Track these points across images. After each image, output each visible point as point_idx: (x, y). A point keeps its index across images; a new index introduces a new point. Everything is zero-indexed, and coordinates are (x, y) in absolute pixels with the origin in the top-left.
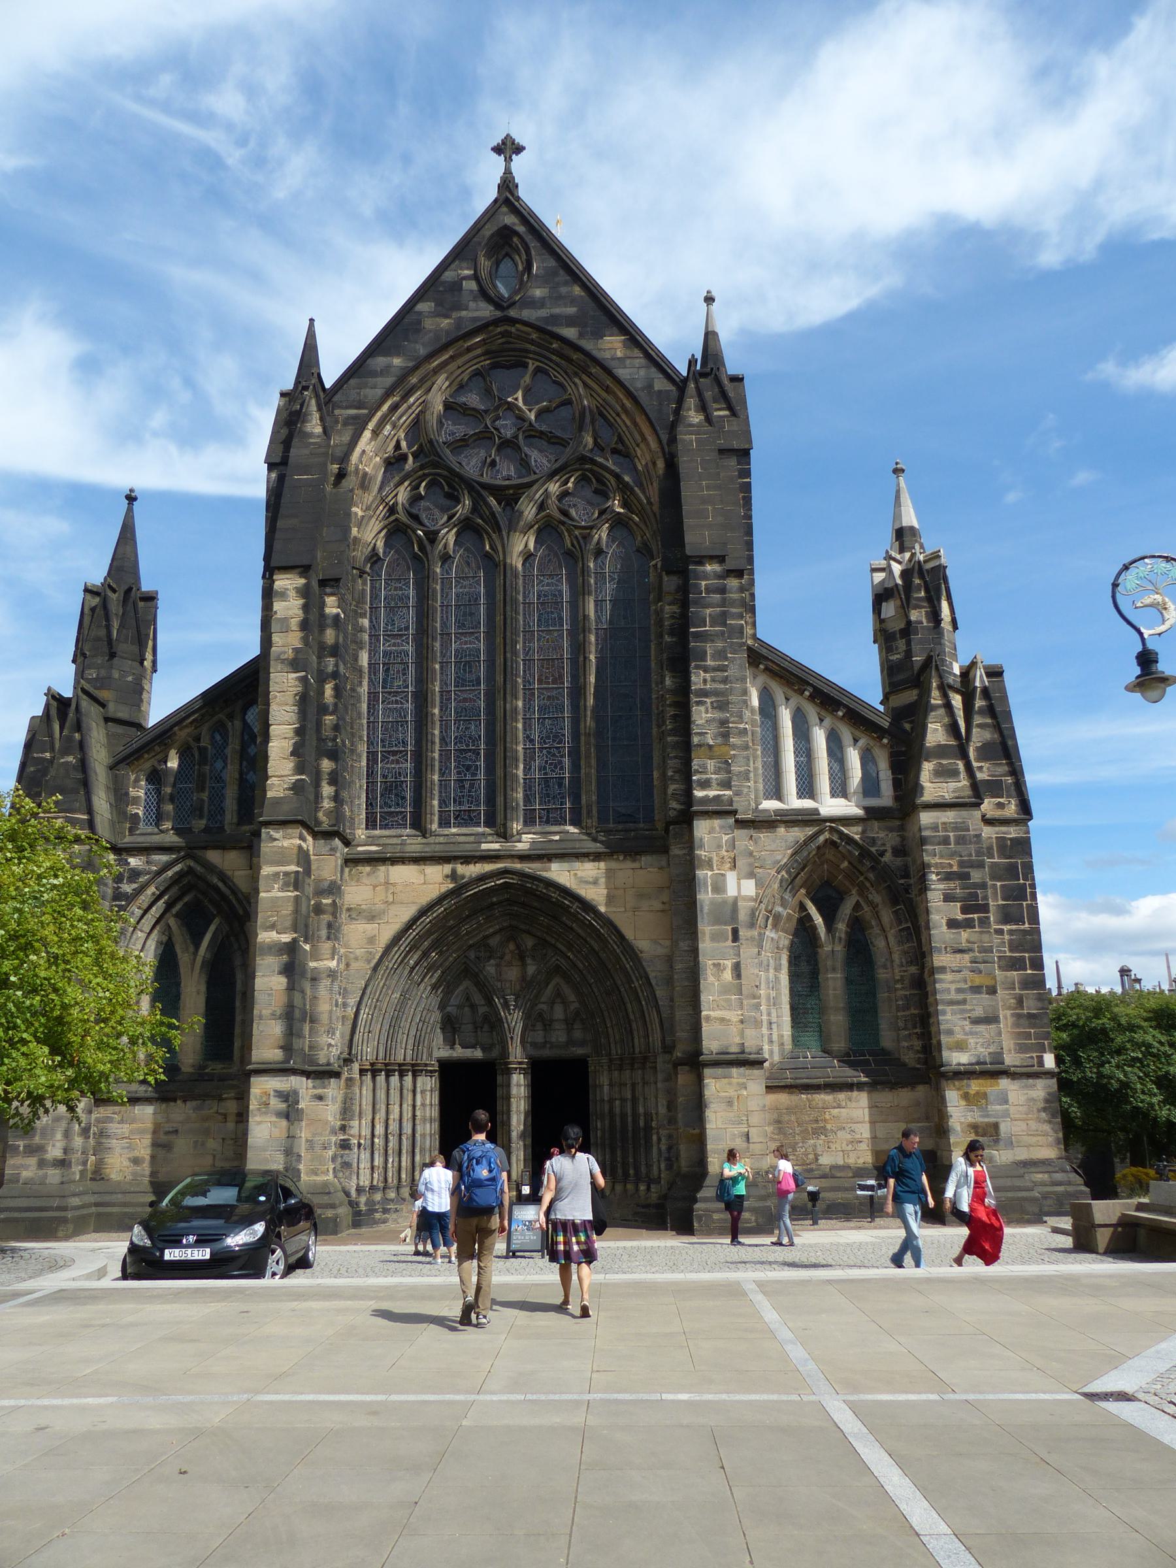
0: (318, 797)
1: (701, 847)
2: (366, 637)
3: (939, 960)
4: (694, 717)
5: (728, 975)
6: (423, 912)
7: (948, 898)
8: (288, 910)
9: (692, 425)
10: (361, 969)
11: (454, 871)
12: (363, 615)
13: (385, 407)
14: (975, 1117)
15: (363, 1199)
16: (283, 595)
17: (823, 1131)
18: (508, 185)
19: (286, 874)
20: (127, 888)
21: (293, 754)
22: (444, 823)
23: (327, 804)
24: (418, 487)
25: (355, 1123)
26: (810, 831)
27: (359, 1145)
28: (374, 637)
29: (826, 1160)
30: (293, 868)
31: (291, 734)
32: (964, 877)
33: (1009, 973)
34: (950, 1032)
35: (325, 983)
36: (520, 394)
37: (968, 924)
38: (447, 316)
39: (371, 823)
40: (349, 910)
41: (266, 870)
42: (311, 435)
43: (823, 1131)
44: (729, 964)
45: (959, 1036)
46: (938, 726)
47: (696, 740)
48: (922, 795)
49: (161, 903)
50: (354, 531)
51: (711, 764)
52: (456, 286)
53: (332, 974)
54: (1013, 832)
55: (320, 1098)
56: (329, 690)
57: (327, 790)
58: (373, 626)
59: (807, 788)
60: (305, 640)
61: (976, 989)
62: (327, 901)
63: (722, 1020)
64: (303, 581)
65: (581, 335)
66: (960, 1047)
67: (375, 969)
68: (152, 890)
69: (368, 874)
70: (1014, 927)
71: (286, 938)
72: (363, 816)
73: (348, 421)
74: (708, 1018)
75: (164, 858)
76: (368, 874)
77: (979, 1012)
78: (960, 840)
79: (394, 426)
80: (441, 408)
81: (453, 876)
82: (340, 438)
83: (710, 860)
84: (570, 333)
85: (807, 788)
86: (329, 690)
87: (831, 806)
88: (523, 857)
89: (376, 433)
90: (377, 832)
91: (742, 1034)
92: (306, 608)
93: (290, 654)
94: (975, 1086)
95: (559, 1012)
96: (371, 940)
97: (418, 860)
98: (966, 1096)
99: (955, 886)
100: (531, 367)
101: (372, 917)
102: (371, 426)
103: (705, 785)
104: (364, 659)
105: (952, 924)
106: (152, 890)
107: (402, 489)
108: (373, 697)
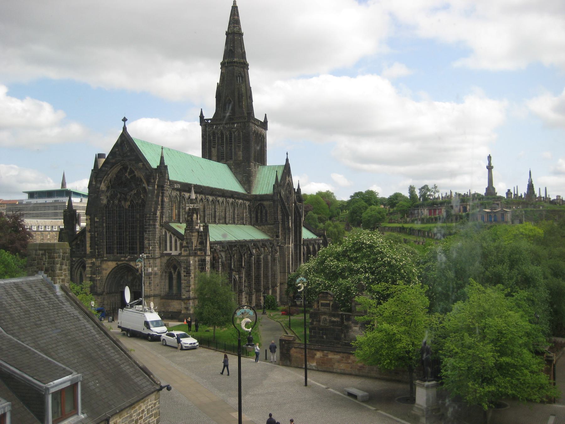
0: (95, 252)
2: (105, 221)
3: (182, 282)
5: (148, 284)
6: (113, 269)
7: (184, 272)
9: (152, 183)
10: (105, 278)
12: (104, 217)
13: (105, 178)
14: (185, 306)
15: (107, 312)
17: (169, 306)
18: (125, 129)
20: (73, 263)
22: (117, 254)
23: (97, 253)
26: (170, 257)
28: (106, 221)
29: (170, 310)
30: (90, 265)
32: (186, 268)
34: (183, 293)
35: (98, 281)
36: (127, 173)
37: (187, 276)
39: (107, 254)
41: (87, 265)
42: (93, 185)
43: (169, 306)
44: (148, 282)
45: (184, 294)
47: (145, 246)
49: (79, 265)
50: (102, 201)
51: (147, 250)
53: (99, 280)
55: (98, 298)
56: (96, 234)
57: (97, 251)
58: (106, 219)
59: (171, 249)
60: (91, 227)
61: (187, 286)
62: (98, 269)
63: (147, 291)
66: (184, 295)
67: (107, 278)
68: (77, 264)
71: (90, 276)
72: (105, 252)
75: (78, 259)
77: (187, 290)
78: (187, 262)
79: (107, 181)
81: (117, 264)
82: (98, 185)
85: (171, 249)
87: (174, 253)
88: (127, 261)
89: (104, 182)
90: (108, 255)
91: (150, 293)
92: (90, 222)
93: (89, 230)
94: (186, 302)
95: (137, 284)
96: (106, 273)
97: (112, 261)
98: (184, 303)
99: (185, 270)
100: (129, 168)
101: (106, 270)
102: (103, 182)
106: (77, 264)
107: (109, 193)
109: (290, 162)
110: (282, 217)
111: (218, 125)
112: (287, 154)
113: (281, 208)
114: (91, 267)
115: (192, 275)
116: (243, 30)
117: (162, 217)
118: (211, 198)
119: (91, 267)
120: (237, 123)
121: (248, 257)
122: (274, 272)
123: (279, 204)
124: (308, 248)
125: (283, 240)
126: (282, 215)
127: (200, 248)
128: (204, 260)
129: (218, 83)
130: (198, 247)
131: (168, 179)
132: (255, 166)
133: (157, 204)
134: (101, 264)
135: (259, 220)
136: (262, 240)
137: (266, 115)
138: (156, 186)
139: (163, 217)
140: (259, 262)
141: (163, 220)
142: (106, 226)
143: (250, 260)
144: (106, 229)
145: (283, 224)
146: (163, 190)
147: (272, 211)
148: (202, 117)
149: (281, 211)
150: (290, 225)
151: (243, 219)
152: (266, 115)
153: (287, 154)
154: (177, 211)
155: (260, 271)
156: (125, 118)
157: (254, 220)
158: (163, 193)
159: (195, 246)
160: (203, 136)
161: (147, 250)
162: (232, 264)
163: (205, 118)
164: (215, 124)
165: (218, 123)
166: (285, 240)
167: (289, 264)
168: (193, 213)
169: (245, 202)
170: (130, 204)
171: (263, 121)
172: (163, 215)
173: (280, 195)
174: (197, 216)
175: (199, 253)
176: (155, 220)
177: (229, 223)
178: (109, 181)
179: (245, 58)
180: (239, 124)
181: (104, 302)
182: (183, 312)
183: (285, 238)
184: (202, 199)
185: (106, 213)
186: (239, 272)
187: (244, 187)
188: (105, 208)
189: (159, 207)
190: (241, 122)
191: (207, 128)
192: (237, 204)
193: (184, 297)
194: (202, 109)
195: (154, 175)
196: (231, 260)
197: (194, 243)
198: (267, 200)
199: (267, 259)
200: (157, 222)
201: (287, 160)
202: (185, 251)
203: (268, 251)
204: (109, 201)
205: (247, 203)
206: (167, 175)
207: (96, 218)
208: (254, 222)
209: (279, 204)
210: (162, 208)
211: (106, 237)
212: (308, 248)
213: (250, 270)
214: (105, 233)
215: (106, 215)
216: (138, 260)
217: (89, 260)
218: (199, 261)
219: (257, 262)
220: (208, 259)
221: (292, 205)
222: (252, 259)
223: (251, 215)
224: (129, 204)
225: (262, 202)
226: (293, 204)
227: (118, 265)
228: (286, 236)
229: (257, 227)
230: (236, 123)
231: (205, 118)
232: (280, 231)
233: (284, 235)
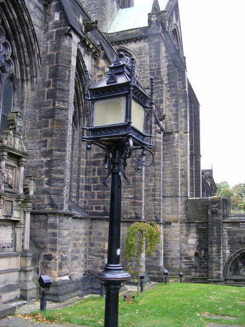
110: (168, 70)
122: (152, 184)
123: (162, 44)
143: (57, 47)
145: (172, 85)
147: (145, 61)
149: (166, 57)
166: (176, 119)
167: (184, 176)
183: (176, 115)
198: (136, 39)
213: (52, 95)
225: (124, 46)
228: (177, 110)
232: (164, 98)
233: (174, 109)
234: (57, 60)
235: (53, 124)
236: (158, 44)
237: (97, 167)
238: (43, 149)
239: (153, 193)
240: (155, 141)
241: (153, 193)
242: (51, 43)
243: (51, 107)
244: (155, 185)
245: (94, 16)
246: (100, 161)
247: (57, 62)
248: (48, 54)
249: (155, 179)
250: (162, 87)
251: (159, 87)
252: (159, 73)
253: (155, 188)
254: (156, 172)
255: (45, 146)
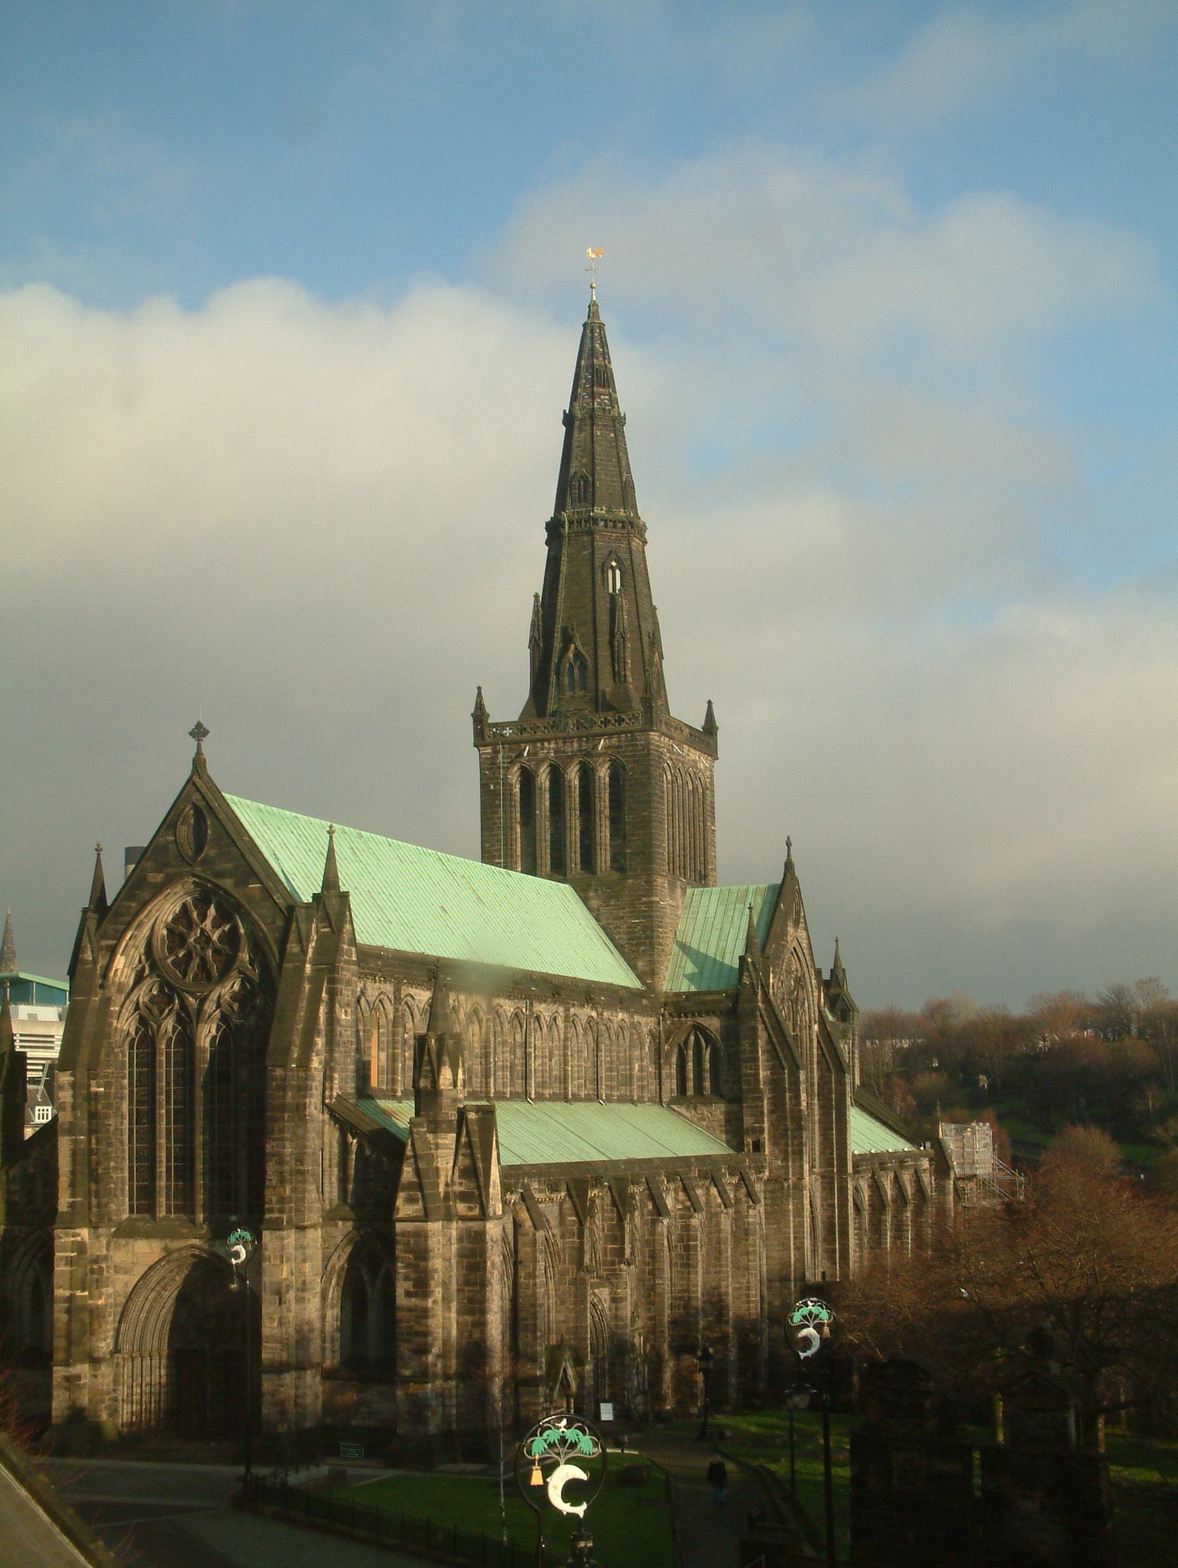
1: (266, 1249)
4: (268, 1169)
7: (406, 1279)
8: (68, 1276)
11: (166, 1245)
12: (124, 1077)
16: (62, 1088)
18: (199, 764)
19: (67, 1257)
21: (70, 1186)
24: (151, 991)
25: (121, 1388)
27: (123, 1400)
28: (131, 1092)
31: (69, 1174)
33: (466, 1317)
38: (159, 872)
39: (131, 1211)
40: (115, 1266)
41: (58, 1254)
42: (87, 962)
46: (410, 1169)
48: (398, 1214)
52: (165, 848)
54: (474, 1225)
56: (94, 1141)
58: (131, 1084)
62: (95, 1267)
64: (72, 1079)
65: (236, 884)
69: (124, 1246)
70: (471, 1288)
71: (67, 1293)
72: (127, 1207)
73: (107, 946)
74: (265, 1347)
76: (124, 1246)
80: (165, 932)
81: (165, 1249)
83: (270, 1257)
84: (228, 883)
86: (94, 1141)
92: (74, 1096)
93: (66, 1126)
96: (126, 1285)
97: (147, 1236)
101: (126, 1272)
103: (271, 1211)
104: (125, 1107)
105: (408, 1294)
108: (131, 1130)
109: (798, 873)
111: (539, 745)
112: (789, 844)
113: (770, 1041)
114: (70, 1262)
115: (438, 1292)
116: (624, 407)
117: (328, 1077)
118: (508, 1007)
119: (70, 1262)
120: (610, 735)
121: (645, 1223)
122: (744, 1281)
123: (760, 1027)
124: (876, 1187)
125: (776, 1158)
126: (772, 1068)
127: (463, 1189)
128: (479, 1237)
129: (536, 596)
130: (457, 1188)
131: (353, 941)
132: (672, 887)
133: (311, 1029)
134: (108, 1250)
135: (690, 1085)
136: (701, 1159)
137: (710, 703)
138: (308, 966)
139: (332, 1079)
140: (689, 1240)
141: (331, 1089)
142: (131, 1114)
143: (653, 1232)
144: (131, 1123)
146: (332, 981)
148: (480, 716)
150: (804, 1104)
151: (631, 1084)
152: (710, 703)
153: (789, 844)
154: (383, 1055)
155: (692, 1276)
156: (199, 725)
157: (670, 1085)
158: (332, 993)
159: (447, 1185)
160: (484, 786)
161: (274, 1199)
162: (587, 1247)
163: (490, 721)
164: (527, 742)
165: (539, 735)
168: (440, 1064)
169: (637, 1018)
170: (217, 1031)
171: (698, 723)
172: (332, 1070)
173: (766, 994)
174: (455, 1075)
175: (461, 1208)
176: (303, 1089)
177: (577, 1098)
178: (142, 951)
179: (634, 507)
180: (614, 740)
181: (114, 1390)
182: (400, 1430)
183: (786, 1153)
184: (476, 1012)
185: (131, 1064)
186: (612, 1278)
187: (633, 967)
188: (126, 1047)
189: (320, 1042)
190: (619, 734)
191: (500, 756)
192: (608, 1030)
193: (407, 1373)
194: (479, 688)
195: (303, 926)
196: (581, 1235)
197: (442, 1174)
199: (719, 1231)
200: (311, 1096)
201: (789, 866)
202: (410, 1200)
203: (719, 1200)
204: (142, 1021)
205: (647, 1023)
206: (348, 927)
207: (93, 1082)
208: (672, 1091)
209: (760, 1027)
210: (331, 1043)
211: (131, 1149)
212: (876, 1187)
213: (652, 1273)
214: (126, 1138)
215: (131, 1073)
216: (237, 1235)
217: (67, 1235)
218: (460, 1239)
219: (681, 1239)
220: (493, 1229)
221: (810, 1027)
222: (659, 1229)
223: (659, 1068)
224: (214, 1032)
226: (816, 1027)
227: (168, 1252)
229: (683, 1110)
230: (602, 735)
231: (490, 721)
232: (766, 1125)
234: (654, 1243)
235: (654, 1296)
236: (755, 1029)
237: (682, 1303)
238: (648, 1315)
239: (747, 1292)
240: (748, 1223)
241: (747, 1292)
242: (648, 1229)
243: (652, 1282)
244: (748, 1283)
245: (643, 951)
246: (684, 1297)
247: (654, 1247)
248: (646, 1237)
249: (749, 1273)
250: (763, 1106)
251: (757, 1106)
252: (757, 1081)
253: (749, 1287)
254: (750, 1263)
255: (650, 1312)
